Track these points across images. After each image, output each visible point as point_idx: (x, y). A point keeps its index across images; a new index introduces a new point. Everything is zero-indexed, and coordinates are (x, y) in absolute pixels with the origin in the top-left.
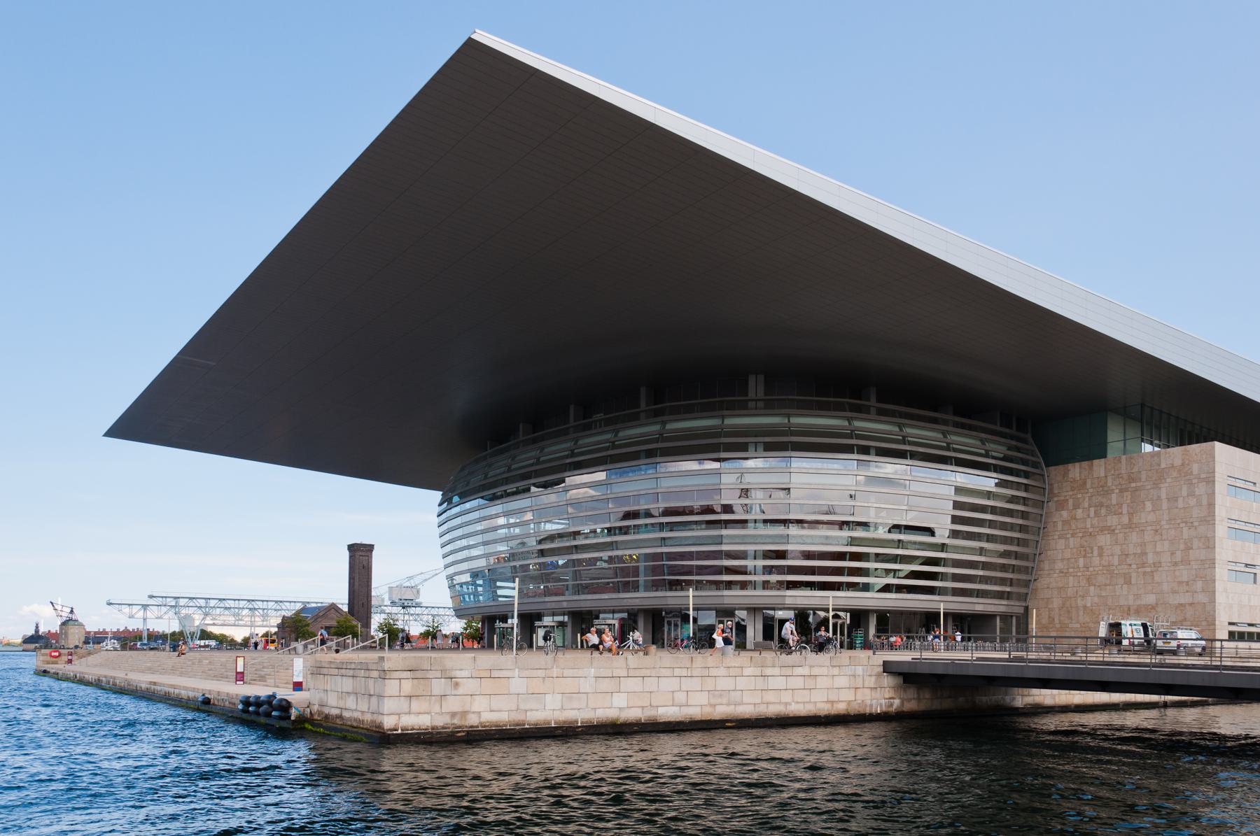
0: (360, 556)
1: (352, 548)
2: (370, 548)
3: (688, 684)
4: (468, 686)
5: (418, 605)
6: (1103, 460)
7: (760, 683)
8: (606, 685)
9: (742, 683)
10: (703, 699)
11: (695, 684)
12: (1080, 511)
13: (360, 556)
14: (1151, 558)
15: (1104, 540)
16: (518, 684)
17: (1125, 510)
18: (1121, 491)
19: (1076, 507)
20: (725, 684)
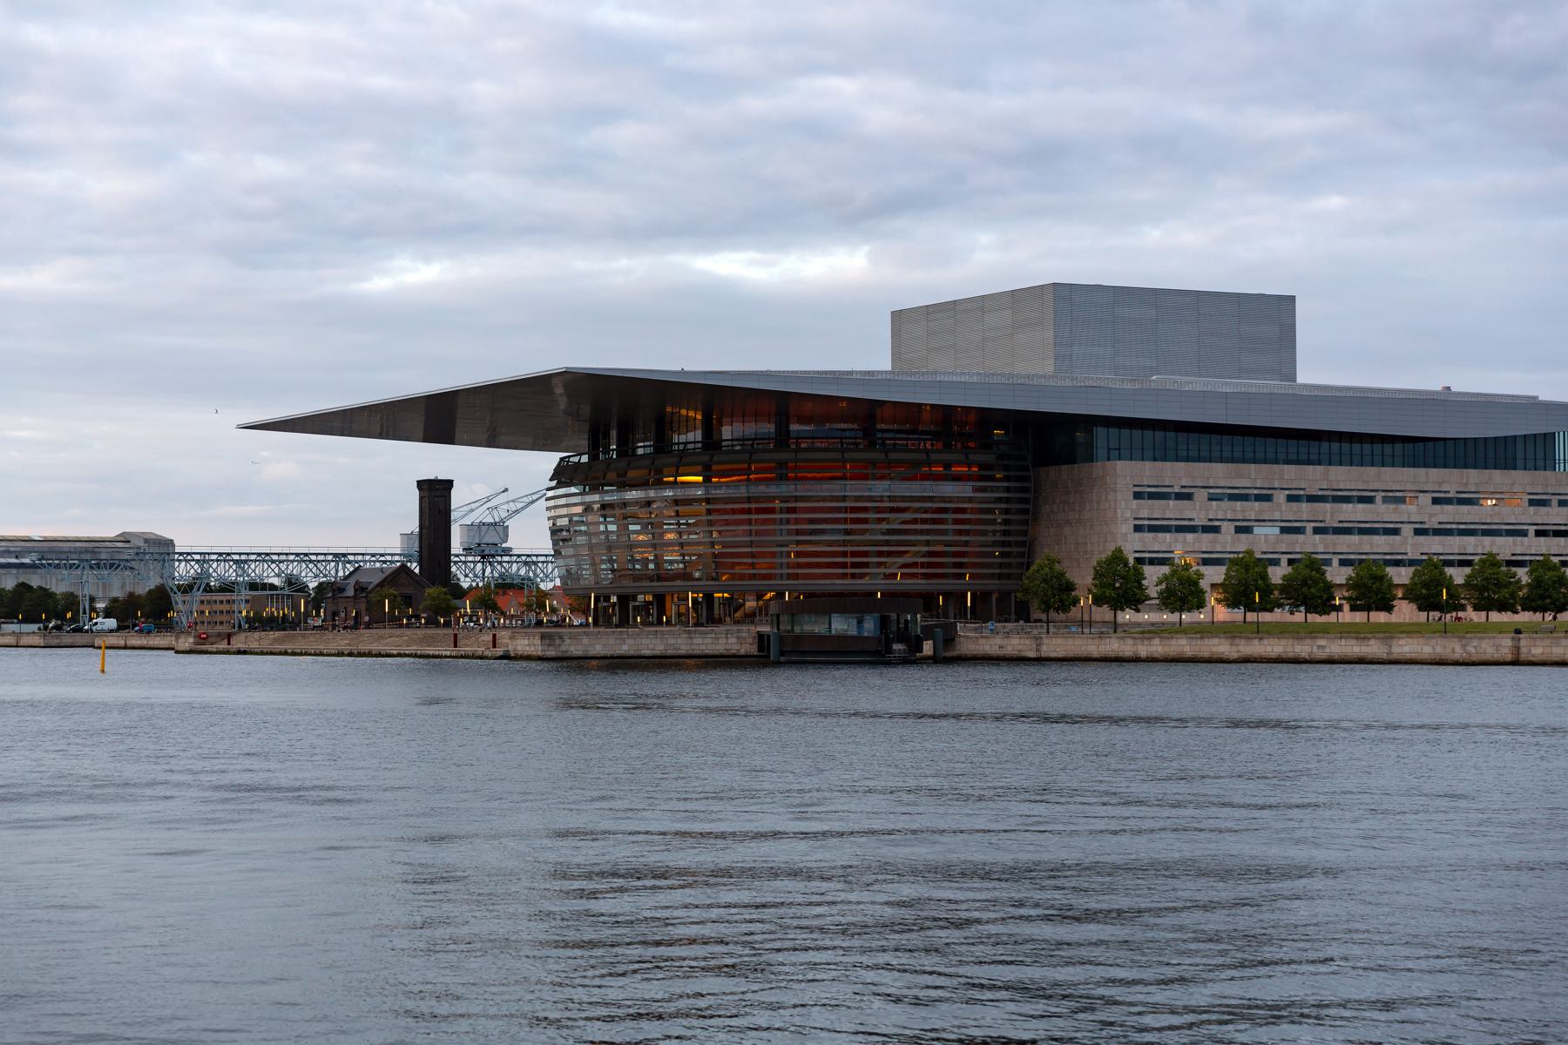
0: (435, 495)
1: (421, 484)
2: (448, 485)
3: (654, 641)
4: (568, 641)
5: (507, 552)
6: (1076, 465)
7: (689, 641)
8: (618, 642)
9: (679, 641)
10: (662, 647)
11: (659, 641)
12: (1055, 506)
13: (435, 495)
14: (1089, 547)
15: (1067, 530)
16: (586, 641)
17: (1077, 508)
18: (1076, 492)
19: (1054, 503)
20: (671, 641)
